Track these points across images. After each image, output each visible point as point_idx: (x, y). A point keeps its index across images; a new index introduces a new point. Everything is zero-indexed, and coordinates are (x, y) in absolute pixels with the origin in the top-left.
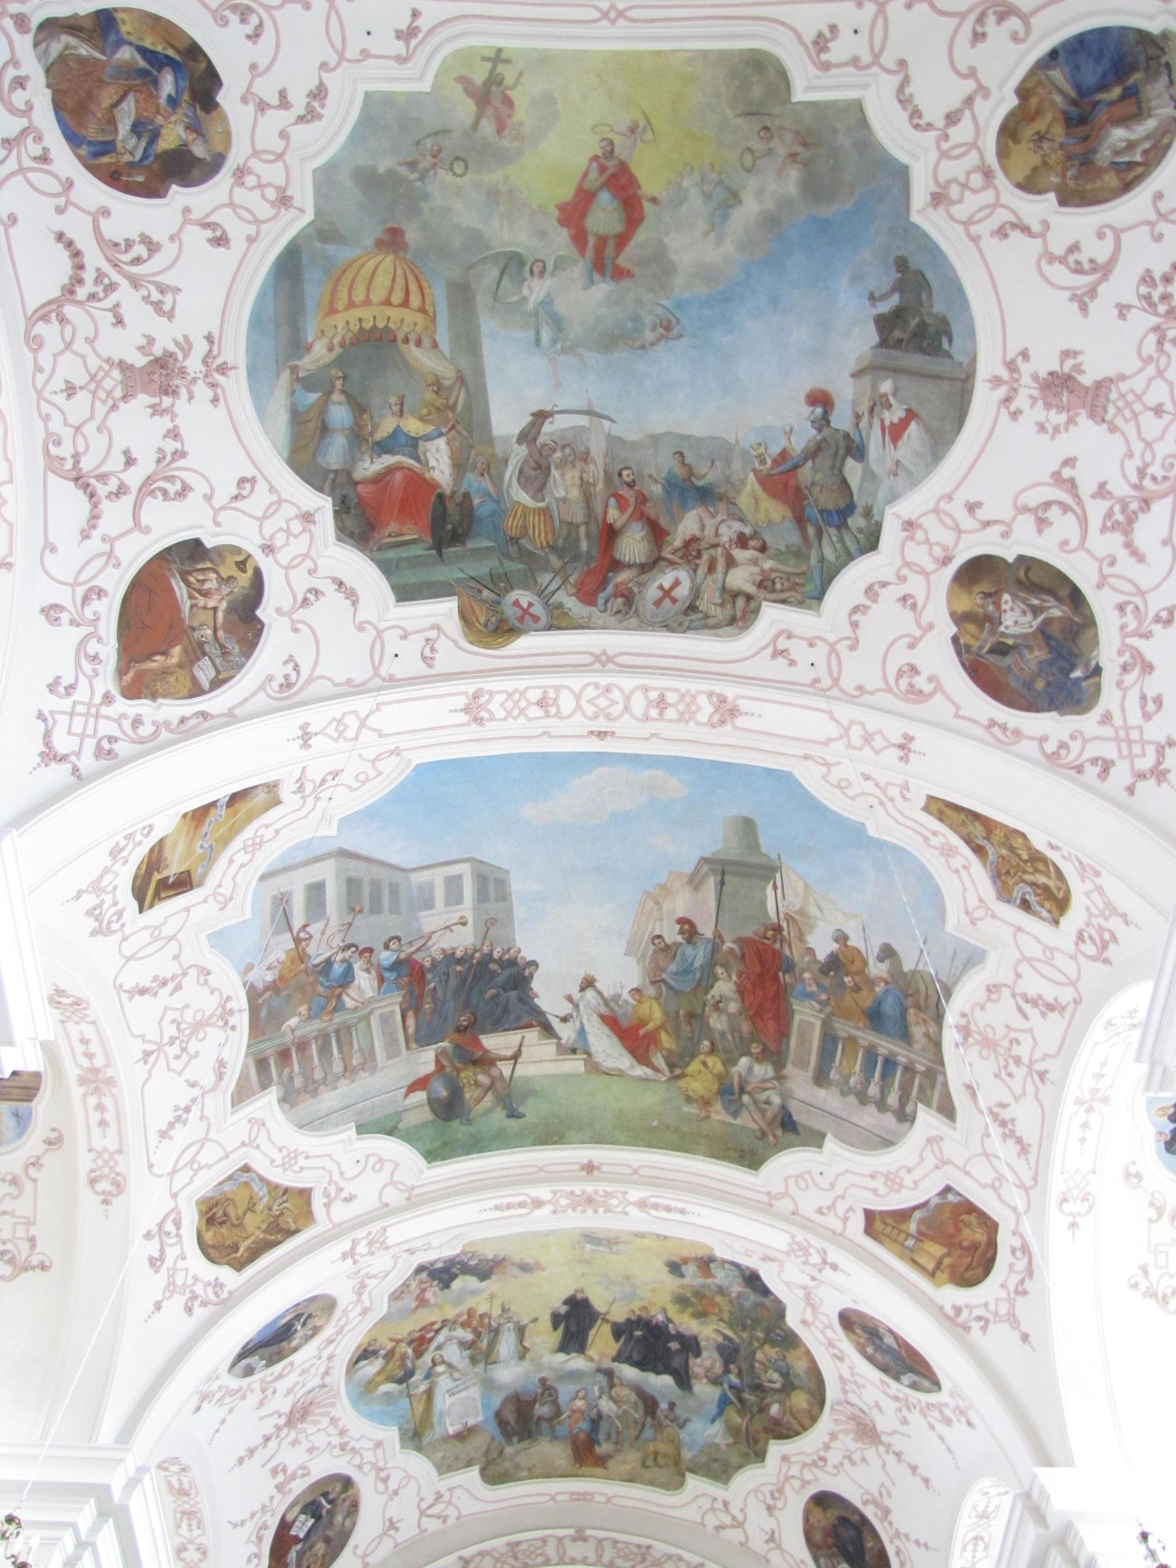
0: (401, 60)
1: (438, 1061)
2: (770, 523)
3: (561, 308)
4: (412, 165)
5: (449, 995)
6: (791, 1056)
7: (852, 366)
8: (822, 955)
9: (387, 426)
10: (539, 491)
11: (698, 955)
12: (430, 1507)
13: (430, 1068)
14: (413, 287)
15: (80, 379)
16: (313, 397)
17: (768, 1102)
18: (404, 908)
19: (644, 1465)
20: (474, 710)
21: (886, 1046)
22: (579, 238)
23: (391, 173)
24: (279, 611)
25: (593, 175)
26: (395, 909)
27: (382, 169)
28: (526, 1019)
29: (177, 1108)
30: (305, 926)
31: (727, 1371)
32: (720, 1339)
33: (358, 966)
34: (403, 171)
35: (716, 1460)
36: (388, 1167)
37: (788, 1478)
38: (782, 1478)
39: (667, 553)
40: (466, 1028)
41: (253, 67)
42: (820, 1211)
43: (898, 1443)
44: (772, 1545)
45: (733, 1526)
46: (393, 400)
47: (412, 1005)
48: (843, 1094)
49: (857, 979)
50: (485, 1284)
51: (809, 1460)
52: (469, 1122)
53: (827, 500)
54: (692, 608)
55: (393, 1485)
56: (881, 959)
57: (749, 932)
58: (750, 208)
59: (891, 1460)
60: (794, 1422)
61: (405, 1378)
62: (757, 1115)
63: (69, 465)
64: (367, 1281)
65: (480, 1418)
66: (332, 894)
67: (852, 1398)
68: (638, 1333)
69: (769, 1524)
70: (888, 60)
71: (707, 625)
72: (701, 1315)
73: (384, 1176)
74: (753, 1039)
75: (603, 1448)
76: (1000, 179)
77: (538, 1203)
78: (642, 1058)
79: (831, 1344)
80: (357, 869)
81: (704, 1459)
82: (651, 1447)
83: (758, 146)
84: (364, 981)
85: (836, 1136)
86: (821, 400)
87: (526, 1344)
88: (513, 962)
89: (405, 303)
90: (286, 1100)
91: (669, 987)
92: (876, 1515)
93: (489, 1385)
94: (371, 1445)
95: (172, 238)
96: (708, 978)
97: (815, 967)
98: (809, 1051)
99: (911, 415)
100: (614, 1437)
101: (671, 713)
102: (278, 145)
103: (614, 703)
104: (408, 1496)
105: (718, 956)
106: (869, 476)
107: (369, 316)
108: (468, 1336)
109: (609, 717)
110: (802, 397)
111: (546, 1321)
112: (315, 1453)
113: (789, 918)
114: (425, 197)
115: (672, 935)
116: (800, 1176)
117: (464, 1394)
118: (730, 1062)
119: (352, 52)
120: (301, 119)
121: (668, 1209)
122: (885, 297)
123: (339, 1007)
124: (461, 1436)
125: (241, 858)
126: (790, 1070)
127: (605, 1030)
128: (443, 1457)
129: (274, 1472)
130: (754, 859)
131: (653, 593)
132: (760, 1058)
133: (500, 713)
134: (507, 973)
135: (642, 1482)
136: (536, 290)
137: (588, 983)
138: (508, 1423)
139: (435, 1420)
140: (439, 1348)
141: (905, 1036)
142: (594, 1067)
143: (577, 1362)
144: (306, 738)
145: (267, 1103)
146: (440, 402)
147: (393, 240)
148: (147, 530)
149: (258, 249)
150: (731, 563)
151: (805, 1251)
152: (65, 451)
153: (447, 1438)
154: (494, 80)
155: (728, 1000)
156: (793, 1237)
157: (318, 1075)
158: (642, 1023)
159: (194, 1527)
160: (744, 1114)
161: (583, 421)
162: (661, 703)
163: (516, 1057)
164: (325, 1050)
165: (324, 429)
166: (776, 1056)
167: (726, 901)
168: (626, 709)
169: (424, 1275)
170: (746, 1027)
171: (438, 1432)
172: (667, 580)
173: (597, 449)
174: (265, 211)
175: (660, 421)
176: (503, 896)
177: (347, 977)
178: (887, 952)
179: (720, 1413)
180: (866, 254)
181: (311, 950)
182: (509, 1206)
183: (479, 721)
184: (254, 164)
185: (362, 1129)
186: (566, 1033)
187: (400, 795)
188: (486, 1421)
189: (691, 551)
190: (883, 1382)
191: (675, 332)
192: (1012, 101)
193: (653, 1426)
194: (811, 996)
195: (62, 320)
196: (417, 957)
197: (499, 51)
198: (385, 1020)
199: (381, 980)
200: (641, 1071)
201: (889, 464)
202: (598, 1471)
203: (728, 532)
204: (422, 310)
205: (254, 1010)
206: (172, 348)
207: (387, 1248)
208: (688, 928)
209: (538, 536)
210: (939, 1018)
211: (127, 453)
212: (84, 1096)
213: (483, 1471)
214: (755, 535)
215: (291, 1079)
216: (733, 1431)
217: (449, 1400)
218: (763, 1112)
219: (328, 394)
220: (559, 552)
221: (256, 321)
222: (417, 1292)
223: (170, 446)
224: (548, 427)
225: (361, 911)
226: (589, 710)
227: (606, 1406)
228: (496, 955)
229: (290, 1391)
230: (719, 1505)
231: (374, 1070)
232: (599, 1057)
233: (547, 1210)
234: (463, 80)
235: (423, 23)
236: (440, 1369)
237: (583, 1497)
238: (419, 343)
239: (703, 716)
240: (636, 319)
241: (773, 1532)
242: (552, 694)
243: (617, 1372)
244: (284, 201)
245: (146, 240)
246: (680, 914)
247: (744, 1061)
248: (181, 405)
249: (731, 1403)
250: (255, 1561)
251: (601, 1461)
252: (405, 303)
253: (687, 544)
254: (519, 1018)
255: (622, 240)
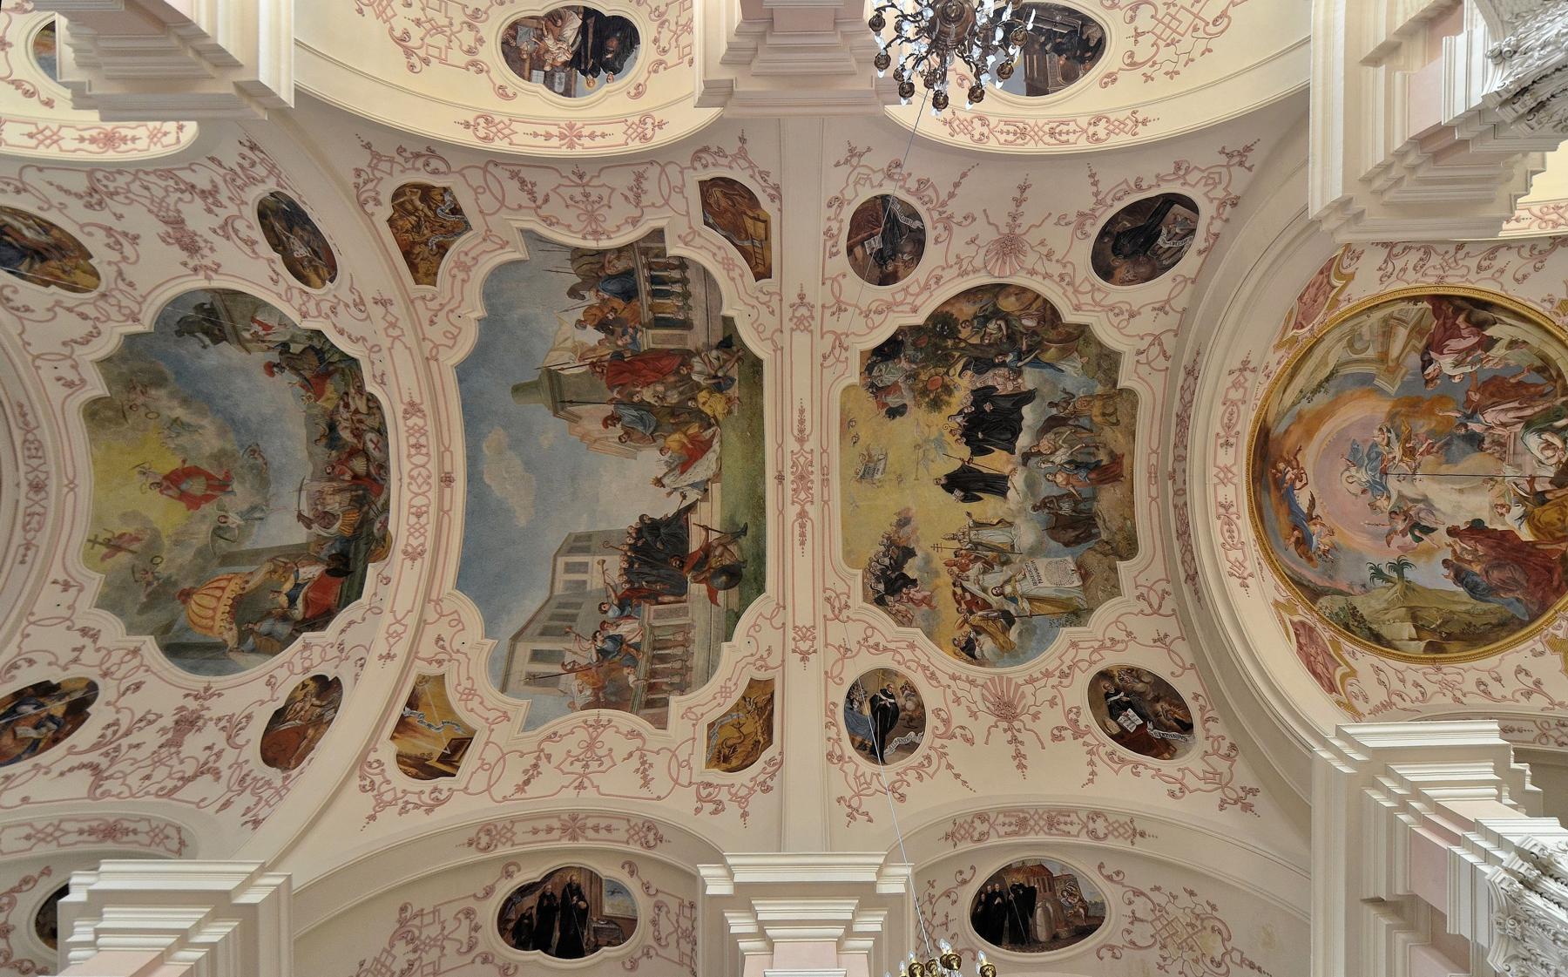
0: (81, 590)
1: (700, 582)
2: (336, 391)
3: (246, 507)
4: (149, 584)
5: (654, 572)
6: (680, 346)
7: (244, 354)
8: (602, 336)
9: (283, 600)
10: (335, 517)
11: (629, 414)
12: (1151, 605)
13: (703, 587)
14: (216, 584)
15: (147, 771)
16: (251, 640)
17: (718, 359)
18: (579, 600)
19: (1117, 423)
20: (413, 555)
21: (644, 287)
22: (207, 498)
23: (148, 595)
24: (337, 667)
25: (170, 492)
26: (578, 606)
27: (143, 599)
28: (682, 522)
29: (637, 771)
30: (563, 665)
31: (1003, 364)
32: (969, 373)
33: (611, 632)
34: (150, 589)
35: (1099, 365)
36: (760, 621)
37: (1097, 304)
38: (1097, 309)
39: (360, 446)
40: (682, 562)
41: (50, 664)
42: (772, 313)
43: (1003, 220)
44: (1167, 308)
45: (1161, 344)
46: (271, 596)
47: (653, 598)
48: (690, 308)
49: (606, 310)
50: (919, 553)
51: (1070, 290)
52: (745, 561)
53: (314, 361)
54: (379, 431)
55: (1123, 636)
56: (583, 297)
57: (603, 384)
58: (179, 412)
59: (1025, 222)
60: (1034, 306)
61: (1009, 619)
62: (729, 365)
63: (181, 783)
64: (871, 642)
65: (1069, 559)
66: (545, 645)
67: (978, 262)
68: (980, 435)
69: (1148, 314)
70: (67, 351)
71: (383, 423)
72: (948, 390)
73: (765, 624)
74: (677, 372)
75: (1103, 457)
76: (102, 288)
77: (803, 514)
78: (707, 445)
79: (926, 287)
80: (537, 627)
81: (1100, 375)
82: (1098, 419)
83: (142, 411)
84: (627, 629)
85: (720, 308)
86: (270, 368)
87: (995, 521)
88: (639, 531)
89: (223, 589)
90: (682, 689)
91: (655, 430)
92: (1093, 225)
93: (1034, 552)
94: (1072, 652)
95: (118, 711)
96: (642, 405)
97: (612, 338)
98: (672, 335)
99: (253, 320)
100: (1092, 450)
101: (423, 441)
102: (103, 652)
103: (419, 474)
104: (1134, 624)
105: (625, 400)
106: (293, 339)
107: (223, 607)
108: (979, 565)
109: (429, 477)
110: (271, 379)
111: (968, 506)
112: (1058, 700)
113: (582, 358)
114: (170, 577)
115: (618, 430)
116: (756, 329)
117: (1042, 572)
118: (699, 387)
119: (67, 614)
120: (95, 642)
121: (802, 422)
122: (202, 341)
123: (637, 647)
124: (1085, 577)
125: (474, 704)
126: (690, 346)
127: (690, 470)
128: (1103, 591)
129: (1055, 738)
130: (546, 383)
131: (376, 454)
132: (691, 368)
133: (421, 540)
134: (646, 534)
135: (1134, 425)
136: (234, 520)
137: (659, 482)
138: (1077, 536)
139: (1064, 596)
140: (984, 590)
141: (629, 273)
142: (717, 477)
143: (1018, 481)
144: (389, 656)
145: (677, 703)
146: (280, 571)
147: (186, 595)
148: (248, 742)
149: (155, 668)
150: (357, 411)
151: (801, 319)
152: (170, 784)
153: (1085, 587)
154: (107, 543)
155: (655, 391)
156: (792, 330)
157: (677, 665)
158: (683, 446)
159: (1068, 819)
160: (731, 373)
161: (304, 494)
162: (418, 446)
163: (707, 529)
164: (663, 659)
165: (269, 634)
166: (686, 356)
167: (580, 399)
168: (423, 466)
169: (889, 599)
170: (671, 379)
171: (1077, 594)
172: (371, 446)
173: (317, 486)
174: (136, 662)
175: (302, 453)
176: (589, 536)
177: (618, 640)
178: (574, 292)
179: (1051, 366)
180: (183, 352)
181: (583, 662)
182: (803, 535)
183: (421, 554)
184: (104, 667)
185: (728, 638)
186: (693, 495)
187: (481, 600)
188: (1073, 554)
189: (358, 434)
190: (936, 241)
191: (255, 447)
192: (53, 288)
193: (1077, 418)
194: (634, 339)
195: (107, 778)
196: (620, 592)
197: (89, 541)
198: (658, 615)
199: (629, 617)
200: (716, 445)
201: (282, 329)
202: (1126, 461)
203: (346, 415)
204: (230, 580)
205: (608, 705)
206: (176, 717)
207: (814, 627)
208: (610, 421)
209: (355, 517)
210: (601, 253)
211: (209, 748)
212: (587, 839)
213: (1122, 558)
214: (342, 399)
215: (672, 684)
216: (1065, 353)
217: (1045, 583)
218: (725, 361)
219: (252, 631)
220: (362, 506)
221: (194, 669)
222: (910, 604)
223: (222, 724)
224: (306, 514)
225: (570, 628)
226: (425, 488)
227: (1061, 457)
228: (632, 541)
229: (974, 715)
230: (1143, 358)
231: (691, 626)
232: (710, 474)
233: (808, 507)
234: (104, 558)
235: (61, 577)
236: (1008, 589)
237: (1153, 475)
238: (247, 582)
239: (420, 422)
240: (252, 468)
241: (1154, 309)
242: (414, 510)
243: (1024, 450)
244: (135, 652)
245: (109, 726)
246: (601, 427)
247: (695, 377)
248: (207, 714)
249: (1036, 357)
250: (1141, 768)
251: (1116, 459)
252: (223, 589)
253: (355, 436)
254: (681, 527)
255: (209, 477)
